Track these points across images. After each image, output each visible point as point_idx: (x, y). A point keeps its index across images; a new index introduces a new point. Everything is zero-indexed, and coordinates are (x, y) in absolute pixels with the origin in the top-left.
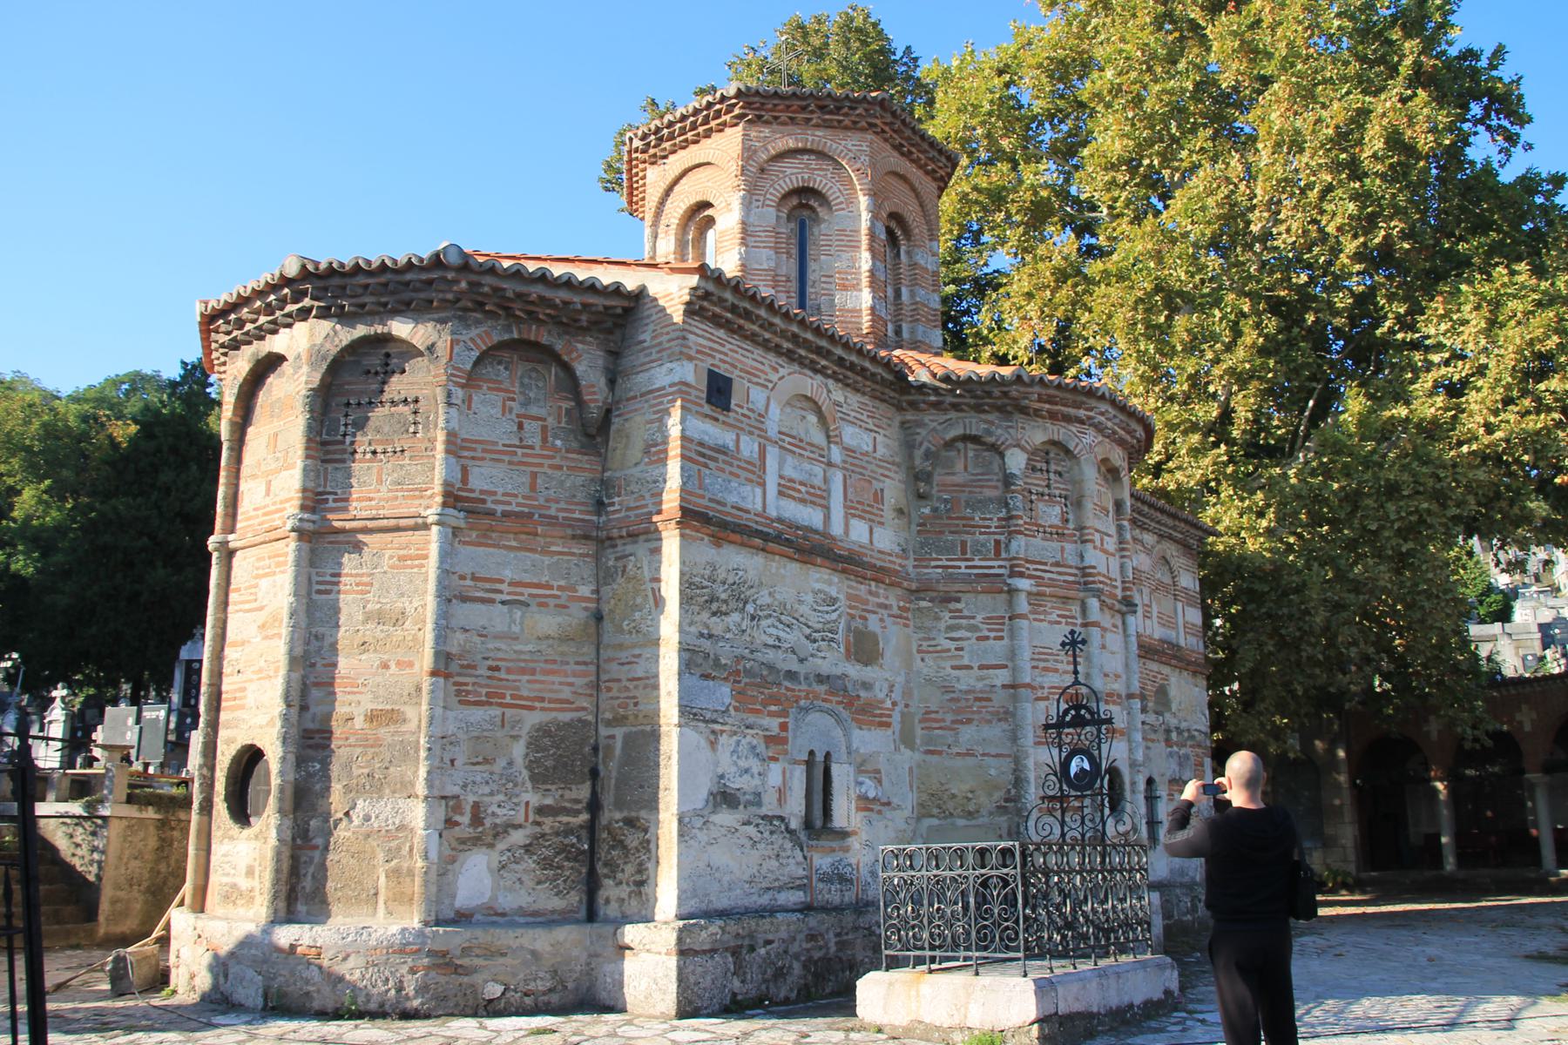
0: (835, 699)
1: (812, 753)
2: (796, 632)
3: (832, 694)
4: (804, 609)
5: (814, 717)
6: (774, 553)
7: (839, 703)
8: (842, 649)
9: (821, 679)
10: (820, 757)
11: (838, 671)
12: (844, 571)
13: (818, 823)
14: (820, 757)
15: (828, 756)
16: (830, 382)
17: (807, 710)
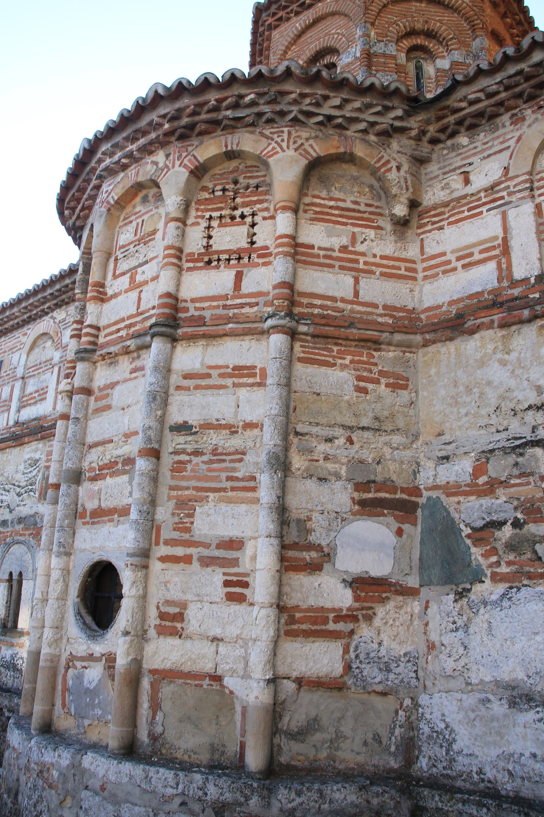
0: (27, 533)
1: (11, 574)
2: (12, 493)
3: (27, 529)
4: (19, 476)
5: (15, 549)
6: (6, 448)
7: (30, 535)
8: (37, 495)
9: (21, 520)
10: (15, 577)
11: (32, 512)
12: (43, 438)
13: (10, 625)
14: (15, 577)
15: (21, 574)
16: (55, 314)
17: (9, 546)
